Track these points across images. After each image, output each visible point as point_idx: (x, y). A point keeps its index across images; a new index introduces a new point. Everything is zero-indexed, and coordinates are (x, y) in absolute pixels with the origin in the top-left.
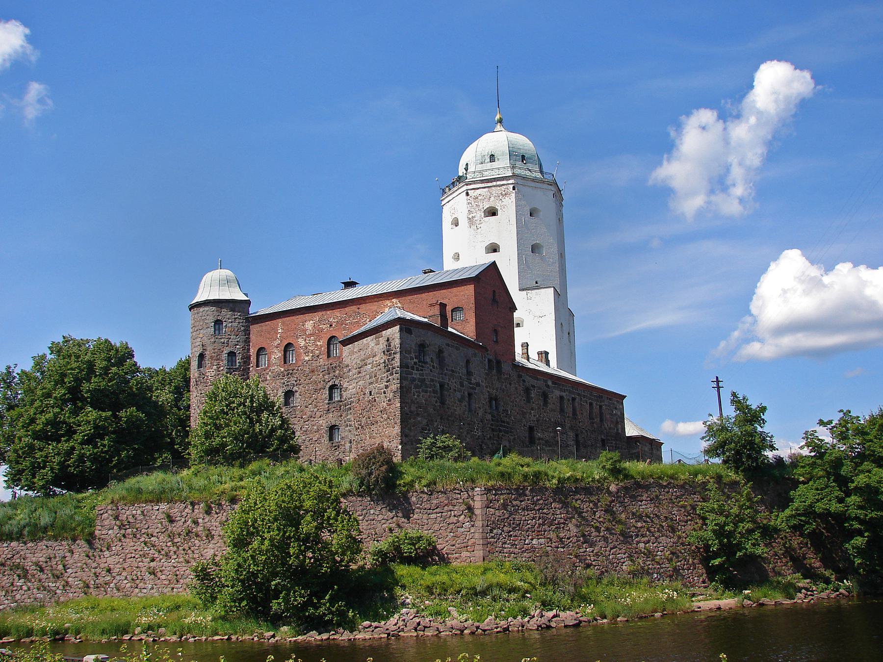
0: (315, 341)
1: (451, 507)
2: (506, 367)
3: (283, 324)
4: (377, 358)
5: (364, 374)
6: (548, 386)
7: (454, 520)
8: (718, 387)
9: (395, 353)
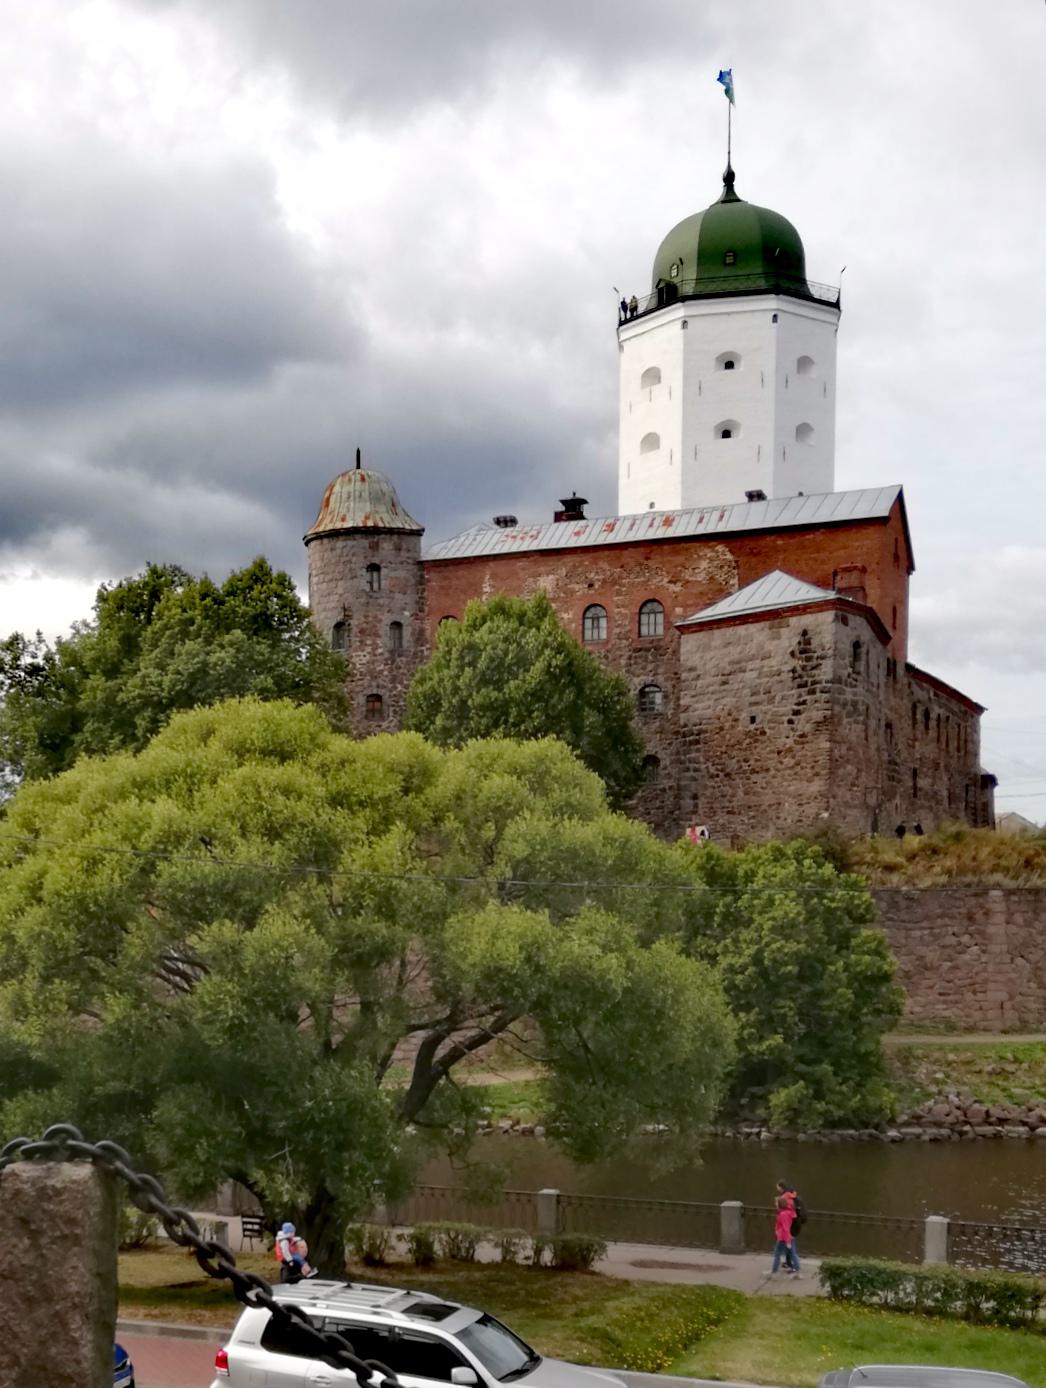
1: (947, 921)
2: (900, 671)
3: (493, 576)
5: (736, 686)
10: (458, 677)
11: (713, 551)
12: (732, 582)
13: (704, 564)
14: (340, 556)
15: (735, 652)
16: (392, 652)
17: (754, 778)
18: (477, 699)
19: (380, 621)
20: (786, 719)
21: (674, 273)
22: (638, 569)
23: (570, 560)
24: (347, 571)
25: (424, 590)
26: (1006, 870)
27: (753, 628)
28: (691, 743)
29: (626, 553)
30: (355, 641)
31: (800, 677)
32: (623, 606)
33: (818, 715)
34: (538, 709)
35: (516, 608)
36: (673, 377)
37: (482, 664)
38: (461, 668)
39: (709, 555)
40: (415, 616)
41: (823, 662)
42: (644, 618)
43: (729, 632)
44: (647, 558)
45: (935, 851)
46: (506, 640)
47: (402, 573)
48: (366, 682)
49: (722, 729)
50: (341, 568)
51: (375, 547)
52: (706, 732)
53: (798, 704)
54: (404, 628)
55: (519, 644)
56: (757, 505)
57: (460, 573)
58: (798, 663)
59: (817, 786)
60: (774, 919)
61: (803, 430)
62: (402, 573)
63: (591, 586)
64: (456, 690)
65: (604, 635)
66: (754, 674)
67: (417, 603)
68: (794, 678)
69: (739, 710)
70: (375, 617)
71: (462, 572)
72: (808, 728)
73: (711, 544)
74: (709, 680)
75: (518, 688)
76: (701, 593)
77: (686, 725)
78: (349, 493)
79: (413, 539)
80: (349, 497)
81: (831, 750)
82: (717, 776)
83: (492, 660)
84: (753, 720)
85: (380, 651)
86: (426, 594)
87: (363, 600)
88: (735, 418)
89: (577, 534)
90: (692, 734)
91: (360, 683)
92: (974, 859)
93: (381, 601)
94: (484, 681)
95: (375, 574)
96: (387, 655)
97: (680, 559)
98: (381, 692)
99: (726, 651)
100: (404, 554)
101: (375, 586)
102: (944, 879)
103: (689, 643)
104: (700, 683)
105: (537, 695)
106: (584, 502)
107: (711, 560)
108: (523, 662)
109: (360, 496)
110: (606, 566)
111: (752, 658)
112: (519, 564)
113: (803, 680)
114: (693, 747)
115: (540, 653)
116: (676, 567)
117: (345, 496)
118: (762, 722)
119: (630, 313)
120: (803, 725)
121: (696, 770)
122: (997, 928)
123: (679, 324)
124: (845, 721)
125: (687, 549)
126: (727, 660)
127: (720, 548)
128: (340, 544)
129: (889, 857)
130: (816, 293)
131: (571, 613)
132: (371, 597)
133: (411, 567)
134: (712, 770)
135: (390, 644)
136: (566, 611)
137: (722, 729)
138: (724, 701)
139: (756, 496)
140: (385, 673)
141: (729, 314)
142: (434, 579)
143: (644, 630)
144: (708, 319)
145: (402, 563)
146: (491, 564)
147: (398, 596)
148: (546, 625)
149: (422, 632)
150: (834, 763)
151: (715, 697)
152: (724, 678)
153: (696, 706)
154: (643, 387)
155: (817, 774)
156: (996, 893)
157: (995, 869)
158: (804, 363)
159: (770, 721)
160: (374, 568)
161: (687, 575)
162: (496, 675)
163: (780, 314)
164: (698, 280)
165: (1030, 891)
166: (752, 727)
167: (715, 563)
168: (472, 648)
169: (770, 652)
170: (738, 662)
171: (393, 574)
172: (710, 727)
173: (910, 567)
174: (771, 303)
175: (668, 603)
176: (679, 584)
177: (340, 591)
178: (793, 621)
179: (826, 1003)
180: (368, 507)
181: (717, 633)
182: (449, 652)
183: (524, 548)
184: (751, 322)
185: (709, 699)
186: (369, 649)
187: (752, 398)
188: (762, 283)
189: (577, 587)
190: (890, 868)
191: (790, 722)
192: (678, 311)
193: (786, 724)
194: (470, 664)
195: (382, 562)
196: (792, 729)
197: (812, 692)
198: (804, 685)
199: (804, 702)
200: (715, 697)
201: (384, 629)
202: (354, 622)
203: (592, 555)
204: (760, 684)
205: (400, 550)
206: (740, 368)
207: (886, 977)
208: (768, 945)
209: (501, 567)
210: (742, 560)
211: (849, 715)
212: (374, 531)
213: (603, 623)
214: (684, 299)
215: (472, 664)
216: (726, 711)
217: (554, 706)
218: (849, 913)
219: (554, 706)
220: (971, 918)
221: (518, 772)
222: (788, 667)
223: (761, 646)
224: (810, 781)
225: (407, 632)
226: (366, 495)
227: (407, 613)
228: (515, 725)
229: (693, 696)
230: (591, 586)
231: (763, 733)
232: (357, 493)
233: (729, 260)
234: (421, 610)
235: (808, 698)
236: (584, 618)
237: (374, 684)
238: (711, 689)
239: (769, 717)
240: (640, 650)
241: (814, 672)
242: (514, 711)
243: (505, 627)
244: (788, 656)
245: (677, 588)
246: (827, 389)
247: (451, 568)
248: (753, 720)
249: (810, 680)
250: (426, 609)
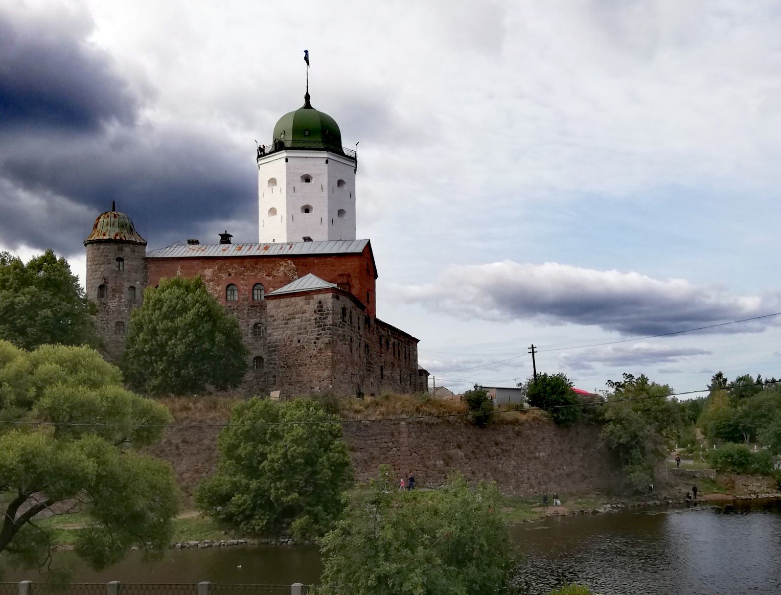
0: (214, 285)
1: (382, 436)
2: (372, 322)
3: (182, 267)
4: (307, 315)
5: (291, 325)
6: (388, 335)
7: (385, 445)
8: (533, 352)
9: (328, 314)
10: (152, 315)
13: (282, 269)
14: (103, 252)
15: (290, 310)
16: (129, 301)
17: (300, 368)
18: (161, 326)
19: (123, 285)
20: (313, 341)
21: (282, 136)
22: (252, 268)
23: (220, 262)
24: (106, 260)
25: (147, 272)
26: (408, 413)
27: (298, 299)
29: (246, 261)
30: (110, 294)
31: (319, 322)
32: (245, 286)
33: (326, 340)
34: (191, 332)
35: (184, 283)
36: (282, 182)
37: (165, 309)
38: (154, 310)
40: (142, 284)
42: (255, 292)
43: (288, 300)
44: (256, 264)
45: (377, 404)
46: (178, 298)
47: (135, 263)
48: (115, 315)
49: (285, 345)
50: (102, 258)
51: (121, 250)
53: (318, 335)
54: (136, 290)
55: (184, 300)
56: (308, 243)
57: (166, 265)
59: (327, 373)
60: (293, 436)
61: (341, 212)
62: (135, 263)
63: (230, 275)
64: (151, 321)
65: (237, 299)
66: (299, 320)
67: (143, 278)
68: (316, 323)
70: (120, 283)
71: (167, 265)
72: (323, 346)
73: (286, 259)
74: (280, 322)
75: (181, 321)
76: (281, 282)
77: (270, 343)
78: (108, 222)
79: (141, 247)
80: (107, 225)
81: (333, 357)
82: (284, 367)
83: (170, 307)
84: (299, 341)
85: (123, 300)
86: (148, 274)
87: (114, 275)
88: (310, 204)
89: (224, 250)
91: (112, 316)
92: (394, 408)
93: (124, 276)
94: (165, 317)
95: (121, 263)
96: (127, 303)
97: (271, 265)
98: (124, 321)
99: (287, 309)
100: (136, 254)
101: (121, 268)
102: (380, 417)
103: (271, 304)
104: (275, 323)
105: (193, 325)
106: (232, 236)
108: (185, 309)
109: (113, 224)
110: (236, 266)
112: (195, 262)
113: (320, 324)
114: (273, 353)
115: (194, 305)
116: (269, 269)
117: (105, 224)
118: (303, 342)
119: (262, 153)
120: (320, 345)
121: (274, 364)
122: (404, 439)
123: (284, 160)
124: (339, 343)
125: (274, 261)
126: (287, 313)
127: (289, 262)
128: (102, 247)
129: (357, 406)
130: (346, 152)
131: (220, 287)
132: (119, 274)
133: (140, 260)
134: (282, 364)
135: (128, 297)
136: (218, 286)
138: (286, 332)
139: (307, 239)
140: (126, 311)
141: (306, 157)
142: (152, 267)
143: (256, 297)
144: (298, 159)
145: (135, 258)
146: (181, 261)
147: (133, 274)
148: (198, 292)
150: (334, 363)
151: (283, 330)
153: (275, 334)
154: (269, 186)
155: (327, 367)
156: (403, 423)
157: (402, 413)
158: (340, 183)
159: (306, 342)
160: (120, 260)
161: (275, 273)
162: (172, 314)
163: (329, 160)
164: (293, 141)
165: (418, 423)
166: (299, 345)
168: (160, 300)
170: (292, 315)
171: (130, 263)
172: (280, 344)
173: (376, 276)
174: (325, 155)
175: (266, 285)
177: (102, 269)
179: (319, 476)
180: (117, 230)
182: (148, 302)
183: (197, 255)
184: (316, 162)
186: (117, 299)
187: (318, 195)
188: (321, 146)
189: (223, 275)
190: (357, 412)
191: (315, 343)
192: (283, 154)
194: (158, 309)
195: (125, 257)
196: (316, 346)
197: (324, 330)
199: (321, 334)
200: (283, 330)
201: (126, 290)
202: (109, 286)
203: (230, 261)
204: (302, 325)
205: (134, 252)
206: (313, 182)
207: (347, 464)
208: (290, 447)
209: (186, 263)
211: (341, 340)
212: (120, 242)
213: (236, 293)
214: (287, 149)
215: (160, 309)
216: (287, 337)
217: (200, 331)
218: (331, 433)
219: (200, 331)
220: (392, 435)
221: (61, 362)
222: (313, 318)
223: (302, 307)
224: (324, 370)
225: (138, 292)
226: (116, 224)
227: (138, 283)
228: (180, 339)
229: (273, 329)
230: (230, 275)
231: (304, 348)
232: (112, 223)
233: (307, 133)
234: (146, 282)
235: (322, 332)
236: (227, 290)
237: (120, 317)
238: (281, 326)
240: (253, 306)
241: (324, 320)
242: (180, 333)
243: (177, 291)
244: (313, 313)
245: (270, 279)
246: (352, 195)
247: (161, 262)
248: (299, 341)
249: (323, 324)
250: (149, 281)
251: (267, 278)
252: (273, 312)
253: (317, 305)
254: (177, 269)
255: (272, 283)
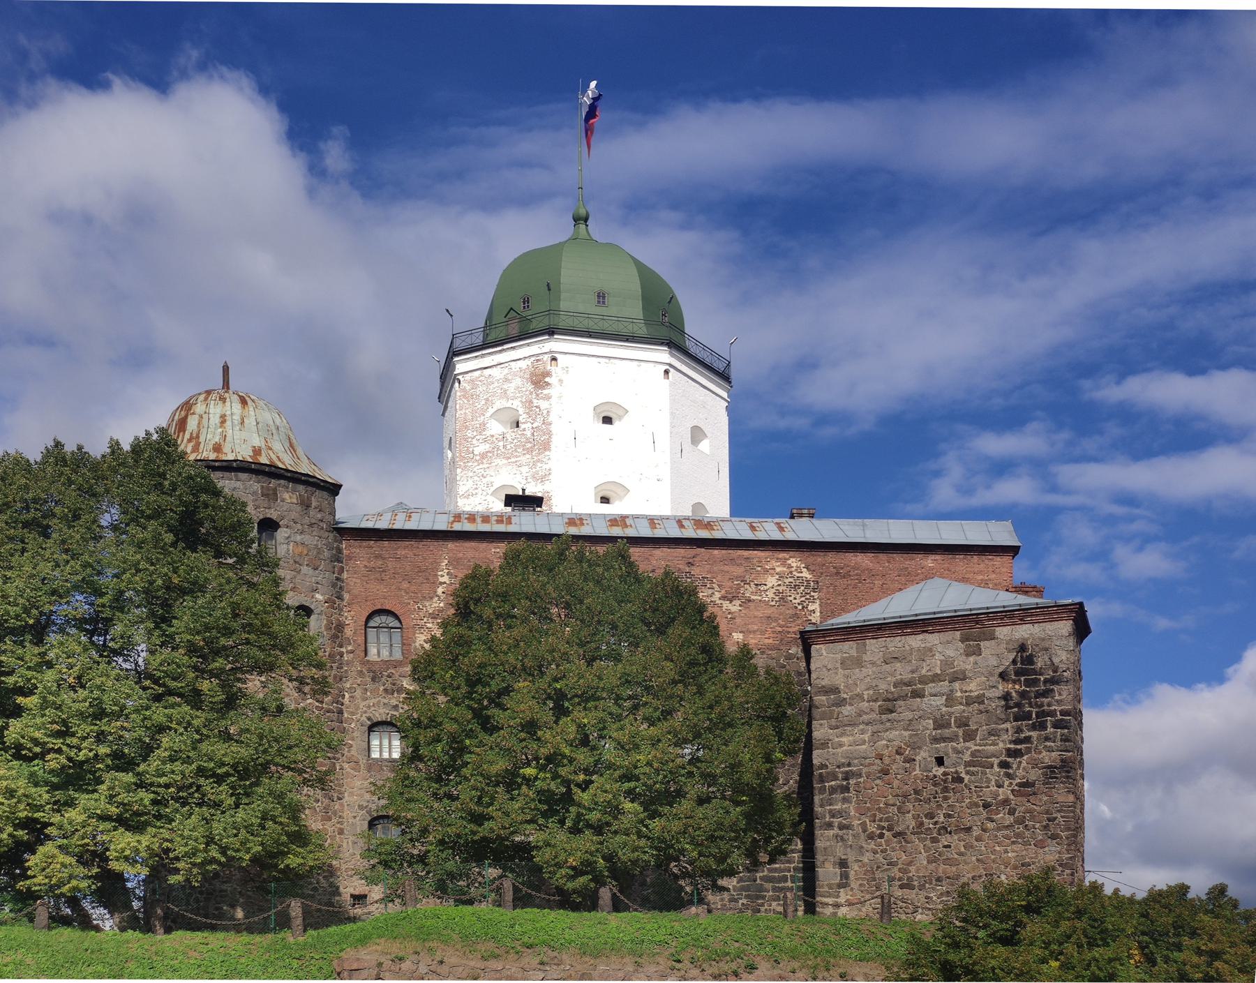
5: (908, 715)
11: (784, 565)
12: (810, 608)
13: (772, 581)
17: (944, 840)
20: (996, 761)
25: (342, 570)
27: (933, 639)
28: (833, 790)
39: (778, 570)
41: (1055, 688)
43: (896, 643)
52: (860, 775)
53: (1016, 742)
58: (1014, 689)
67: (334, 585)
68: (1007, 707)
69: (915, 747)
71: (404, 549)
73: (782, 555)
86: (345, 575)
90: (836, 779)
107: (781, 577)
111: (936, 678)
120: (1023, 769)
127: (794, 562)
137: (886, 772)
142: (359, 555)
149: (340, 627)
151: (875, 728)
152: (890, 704)
153: (844, 739)
159: (968, 764)
161: (749, 591)
167: (787, 581)
169: (964, 672)
176: (737, 602)
178: (1003, 632)
181: (872, 645)
185: (863, 732)
188: (642, 330)
191: (1004, 765)
193: (996, 769)
196: (1008, 776)
198: (1028, 716)
199: (1028, 740)
200: (875, 728)
204: (950, 714)
210: (825, 581)
216: (892, 750)
224: (1040, 845)
227: (319, 596)
231: (961, 780)
234: (340, 598)
239: (967, 757)
244: (996, 678)
245: (735, 607)
250: (346, 596)
251: (726, 604)
252: (838, 679)
253: (1012, 656)
254: (436, 567)
255: (738, 620)
